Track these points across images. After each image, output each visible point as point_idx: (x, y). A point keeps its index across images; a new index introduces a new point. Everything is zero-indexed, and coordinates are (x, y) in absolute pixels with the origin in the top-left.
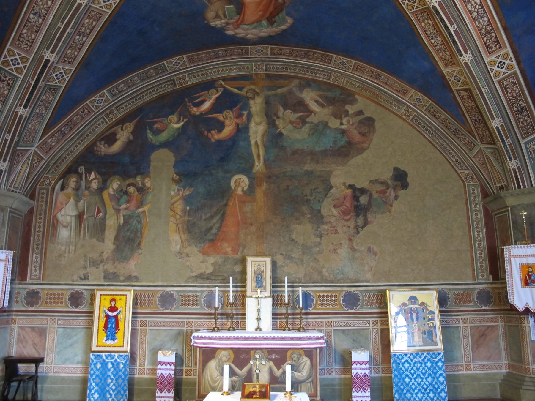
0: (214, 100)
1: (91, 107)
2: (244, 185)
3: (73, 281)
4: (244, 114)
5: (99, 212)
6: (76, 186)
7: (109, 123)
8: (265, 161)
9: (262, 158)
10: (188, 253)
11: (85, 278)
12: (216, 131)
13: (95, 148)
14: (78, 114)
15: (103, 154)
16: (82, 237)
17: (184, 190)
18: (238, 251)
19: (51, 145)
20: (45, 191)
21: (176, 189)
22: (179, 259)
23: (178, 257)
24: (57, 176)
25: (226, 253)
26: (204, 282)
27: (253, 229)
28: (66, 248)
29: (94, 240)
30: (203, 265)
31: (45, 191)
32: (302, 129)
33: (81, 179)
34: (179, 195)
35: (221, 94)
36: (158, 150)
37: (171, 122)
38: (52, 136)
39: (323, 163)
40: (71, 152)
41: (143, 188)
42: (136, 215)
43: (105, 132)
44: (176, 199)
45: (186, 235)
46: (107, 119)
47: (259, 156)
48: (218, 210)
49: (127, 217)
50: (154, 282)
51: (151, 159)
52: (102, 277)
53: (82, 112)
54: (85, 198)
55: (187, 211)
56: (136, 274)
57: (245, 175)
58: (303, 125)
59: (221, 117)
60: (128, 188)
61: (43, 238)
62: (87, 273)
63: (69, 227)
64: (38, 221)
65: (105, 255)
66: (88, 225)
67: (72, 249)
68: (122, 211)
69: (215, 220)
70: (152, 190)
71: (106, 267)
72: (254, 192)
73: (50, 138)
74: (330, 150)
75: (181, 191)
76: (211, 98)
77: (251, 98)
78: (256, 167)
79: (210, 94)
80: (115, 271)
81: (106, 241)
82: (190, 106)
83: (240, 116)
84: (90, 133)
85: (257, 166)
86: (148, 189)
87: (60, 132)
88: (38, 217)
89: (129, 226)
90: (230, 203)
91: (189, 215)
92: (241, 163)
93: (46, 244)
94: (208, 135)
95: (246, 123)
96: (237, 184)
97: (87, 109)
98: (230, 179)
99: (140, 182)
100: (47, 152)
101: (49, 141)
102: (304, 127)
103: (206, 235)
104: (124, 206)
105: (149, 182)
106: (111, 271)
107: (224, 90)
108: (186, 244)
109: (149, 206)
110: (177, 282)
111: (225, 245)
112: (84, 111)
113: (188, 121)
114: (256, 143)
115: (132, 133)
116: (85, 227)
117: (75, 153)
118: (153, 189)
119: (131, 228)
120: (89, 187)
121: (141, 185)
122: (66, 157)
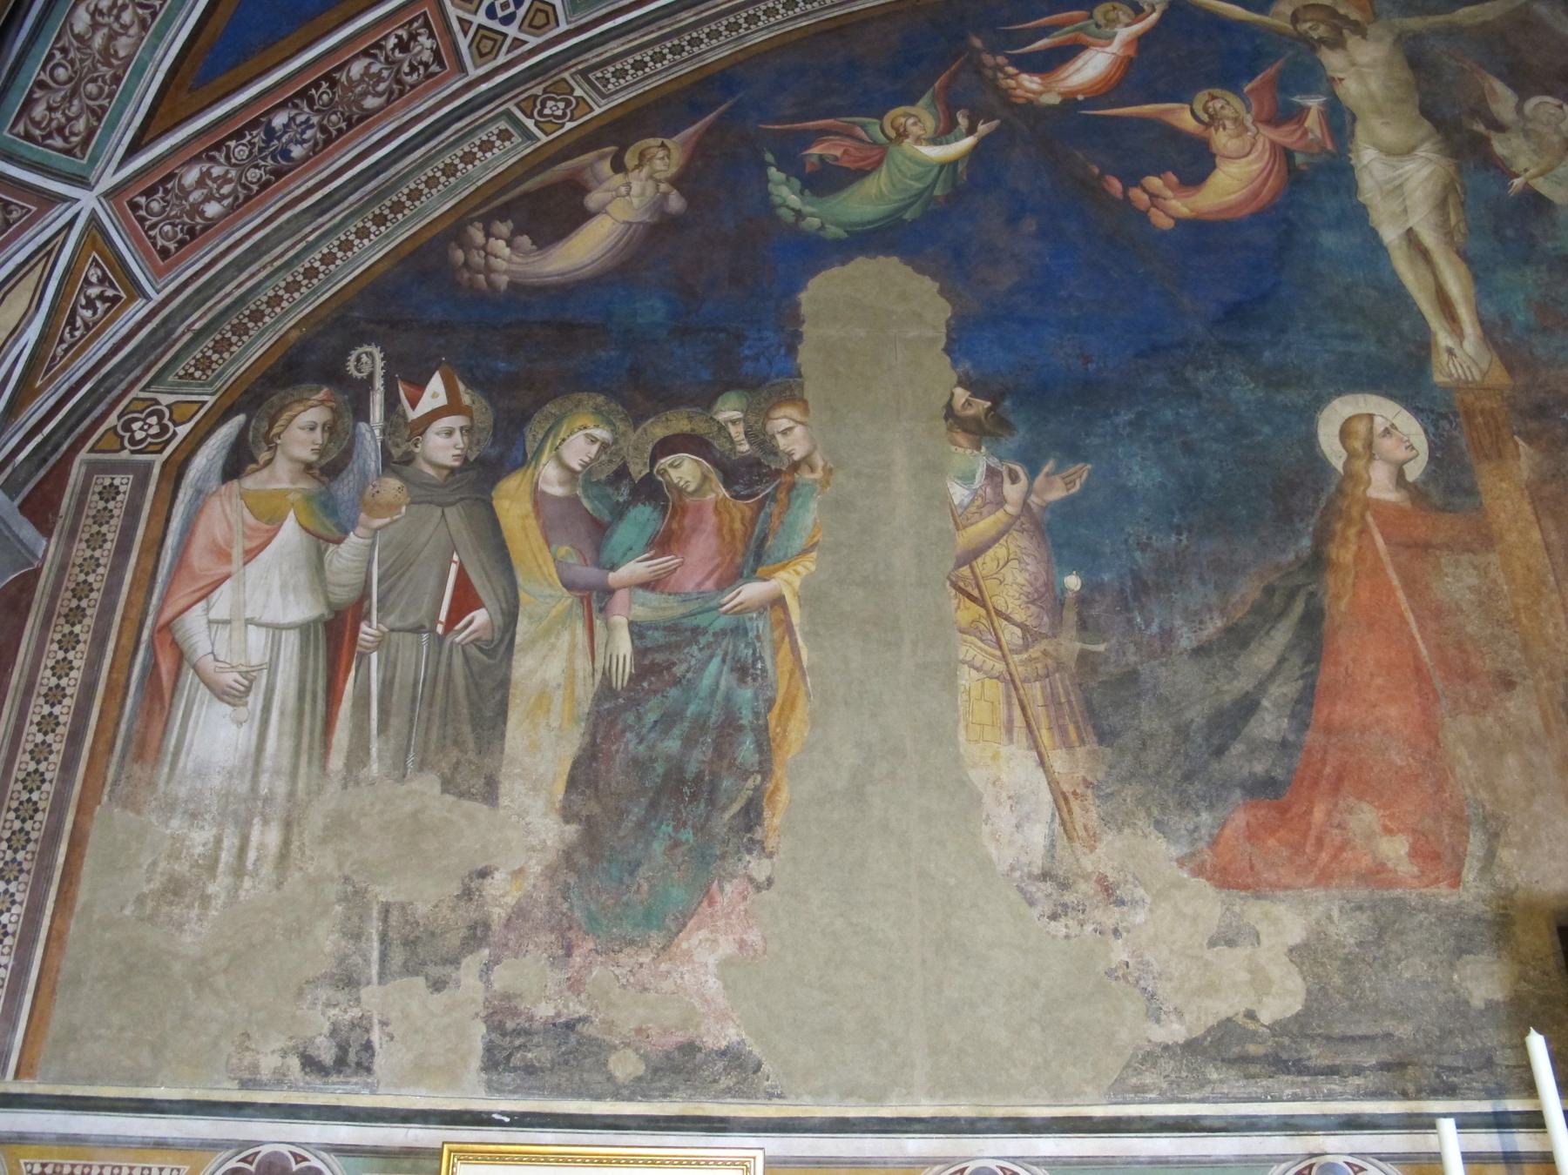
0: (1127, 44)
1: (456, 26)
2: (1401, 454)
3: (244, 1085)
5: (465, 601)
6: (322, 452)
7: (544, 139)
9: (1464, 313)
10: (1112, 877)
11: (341, 1063)
12: (1173, 178)
13: (459, 255)
14: (378, 45)
15: (502, 281)
16: (337, 762)
17: (1033, 472)
18: (1459, 859)
19: (196, 210)
20: (124, 482)
21: (981, 471)
22: (1054, 917)
23: (1046, 907)
24: (211, 400)
25: (1377, 874)
26: (1255, 1088)
27: (1520, 707)
28: (218, 841)
29: (427, 785)
30: (1233, 961)
31: (124, 482)
33: (362, 413)
34: (1000, 502)
36: (843, 264)
37: (902, 135)
38: (211, 146)
40: (311, 273)
41: (759, 464)
42: (722, 622)
43: (519, 181)
44: (986, 525)
45: (1081, 752)
46: (530, 123)
48: (1269, 591)
49: (658, 637)
50: (879, 1098)
51: (805, 309)
52: (476, 1063)
53: (403, 46)
54: (378, 523)
55: (1070, 595)
56: (731, 1034)
57: (1392, 397)
59: (1184, 118)
60: (665, 462)
61: (68, 765)
62: (362, 1025)
63: (255, 700)
64: (53, 654)
65: (501, 894)
66: (387, 685)
67: (262, 846)
68: (621, 597)
69: (1263, 657)
70: (819, 474)
71: (502, 977)
72: (1472, 492)
73: (196, 159)
75: (1014, 479)
76: (1111, 38)
79: (1102, 22)
80: (576, 1009)
81: (512, 791)
82: (1000, 68)
83: (1286, 115)
84: (432, 182)
85: (1450, 352)
86: (795, 466)
87: (258, 136)
88: (60, 629)
89: (674, 692)
90: (1343, 553)
91: (1083, 625)
92: (1355, 337)
93: (84, 809)
95: (1330, 147)
96: (1358, 445)
97: (431, 35)
98: (1308, 415)
99: (737, 432)
100: (165, 253)
101: (192, 176)
103: (1219, 752)
104: (635, 569)
105: (798, 430)
106: (545, 1011)
108: (1087, 814)
109: (807, 565)
110: (1057, 1097)
111: (1365, 817)
112: (413, 37)
113: (998, 130)
114: (1411, 237)
115: (677, 182)
116: (362, 701)
117: (330, 277)
118: (829, 472)
119: (692, 709)
120: (409, 459)
121: (745, 447)
122: (275, 301)
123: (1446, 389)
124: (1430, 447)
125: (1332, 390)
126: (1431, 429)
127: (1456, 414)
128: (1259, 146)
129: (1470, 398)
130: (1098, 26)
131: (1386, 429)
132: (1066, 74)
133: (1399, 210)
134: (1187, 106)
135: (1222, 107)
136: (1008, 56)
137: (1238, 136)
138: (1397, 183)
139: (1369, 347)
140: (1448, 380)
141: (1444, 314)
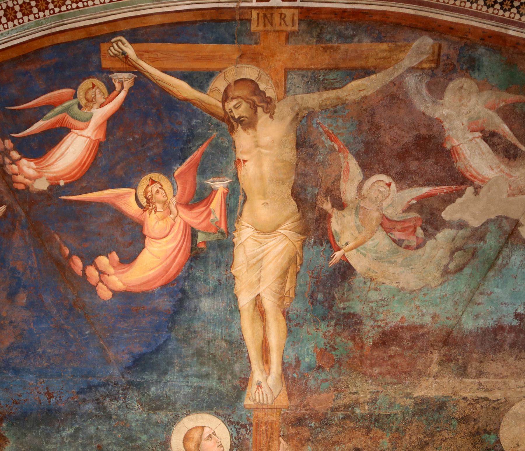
4: (213, 191)
8: (285, 367)
12: (115, 256)
32: (420, 251)
35: (126, 99)
39: (480, 374)
47: (265, 349)
57: (217, 415)
58: (429, 235)
74: (512, 328)
76: (88, 120)
77: (240, 121)
78: (254, 388)
79: (83, 102)
92: (207, 376)
94: (84, 271)
95: (223, 227)
102: (430, 243)
107: (136, 81)
123: (250, 409)
124: (231, 445)
125: (185, 412)
126: (235, 434)
127: (251, 425)
128: (176, 228)
129: (261, 414)
130: (80, 107)
131: (210, 435)
132: (51, 161)
133: (255, 279)
134: (133, 191)
135: (158, 191)
136: (13, 140)
137: (163, 218)
138: (259, 257)
139: (213, 383)
140: (252, 403)
141: (262, 356)
